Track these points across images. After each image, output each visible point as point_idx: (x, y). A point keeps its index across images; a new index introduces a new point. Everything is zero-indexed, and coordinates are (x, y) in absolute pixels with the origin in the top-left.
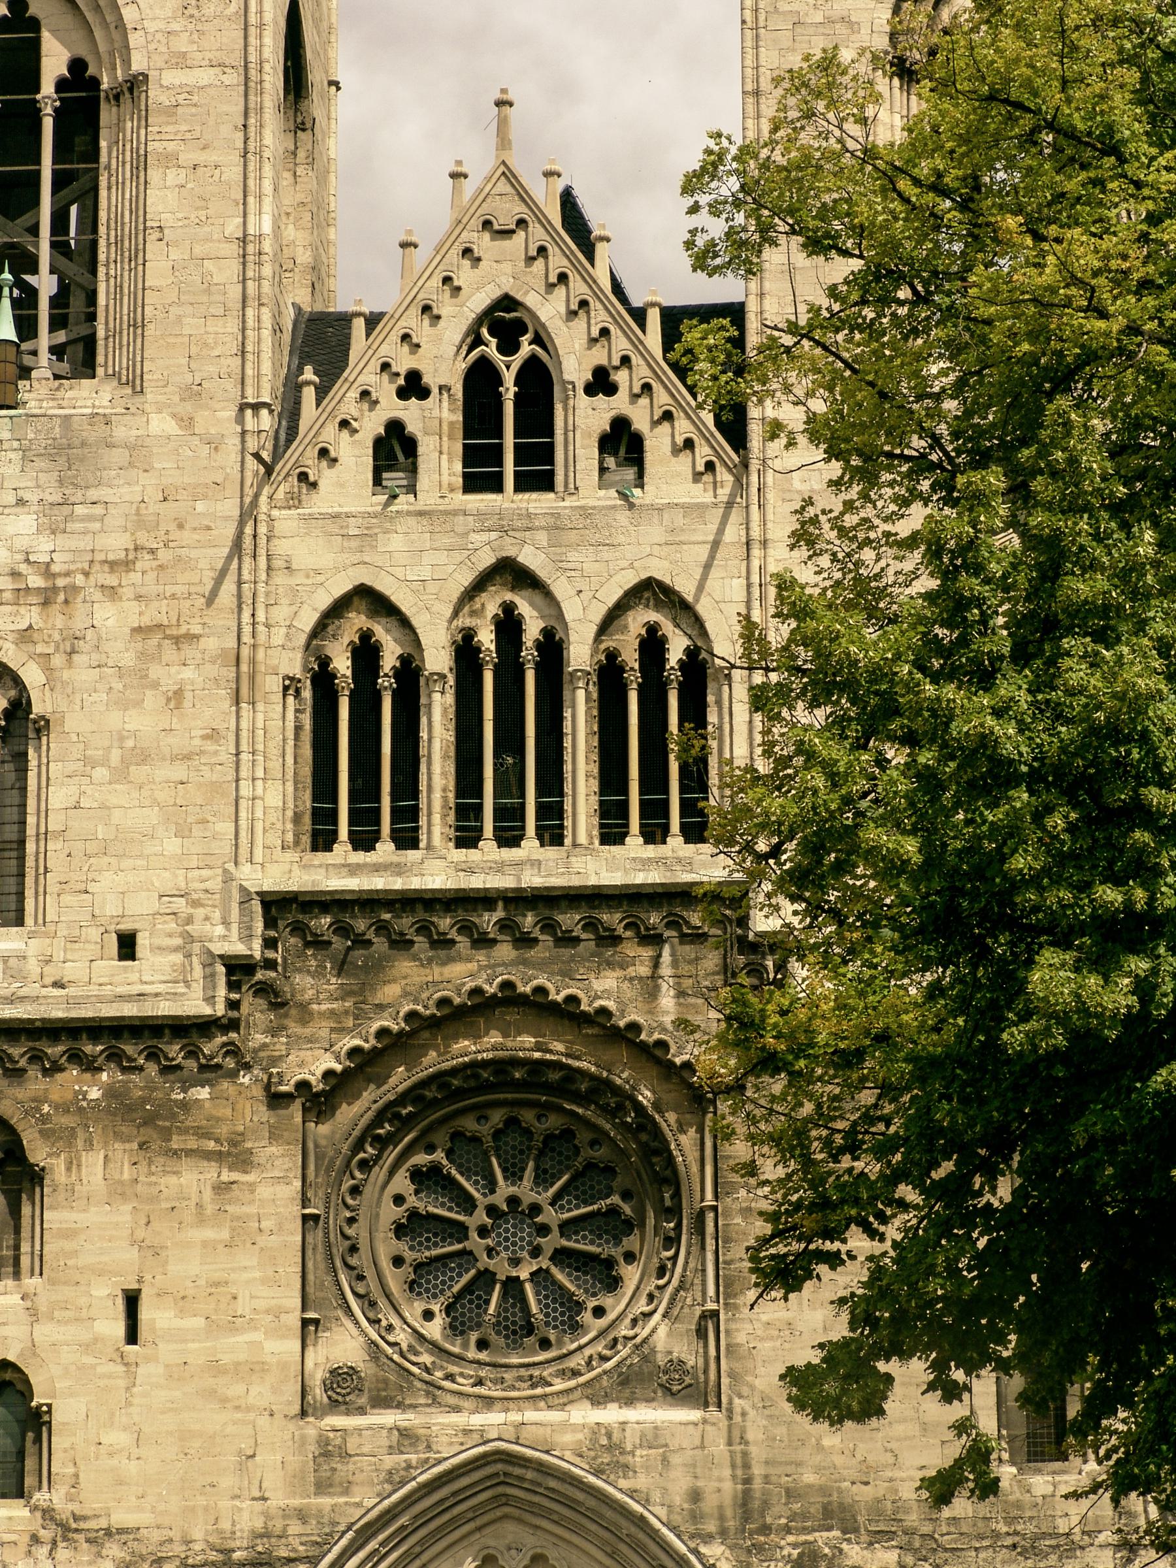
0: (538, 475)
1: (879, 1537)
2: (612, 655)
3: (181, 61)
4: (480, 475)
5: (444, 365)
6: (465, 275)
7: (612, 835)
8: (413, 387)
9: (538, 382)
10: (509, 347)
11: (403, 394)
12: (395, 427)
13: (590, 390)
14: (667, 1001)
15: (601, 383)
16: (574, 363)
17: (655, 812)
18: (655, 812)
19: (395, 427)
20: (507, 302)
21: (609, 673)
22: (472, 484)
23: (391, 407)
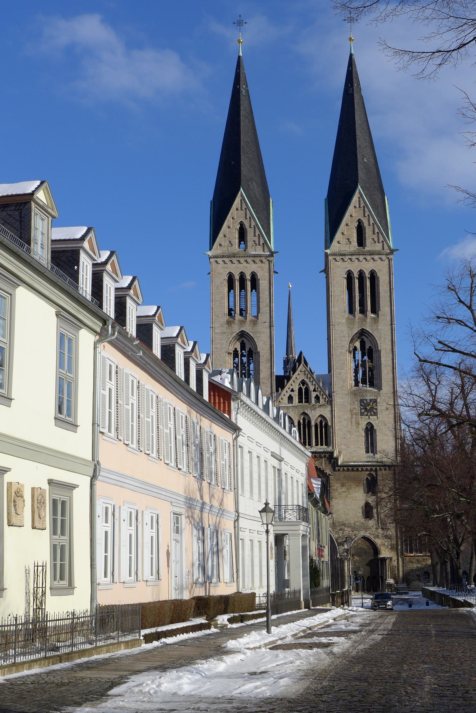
0: (308, 400)
1: (348, 527)
2: (316, 423)
4: (300, 401)
5: (296, 389)
6: (298, 377)
7: (317, 445)
8: (292, 390)
9: (307, 389)
10: (303, 385)
11: (291, 391)
12: (290, 395)
13: (313, 391)
14: (323, 465)
15: (314, 390)
16: (312, 388)
17: (322, 442)
18: (322, 442)
19: (290, 395)
20: (303, 380)
21: (316, 426)
22: (299, 402)
23: (290, 393)
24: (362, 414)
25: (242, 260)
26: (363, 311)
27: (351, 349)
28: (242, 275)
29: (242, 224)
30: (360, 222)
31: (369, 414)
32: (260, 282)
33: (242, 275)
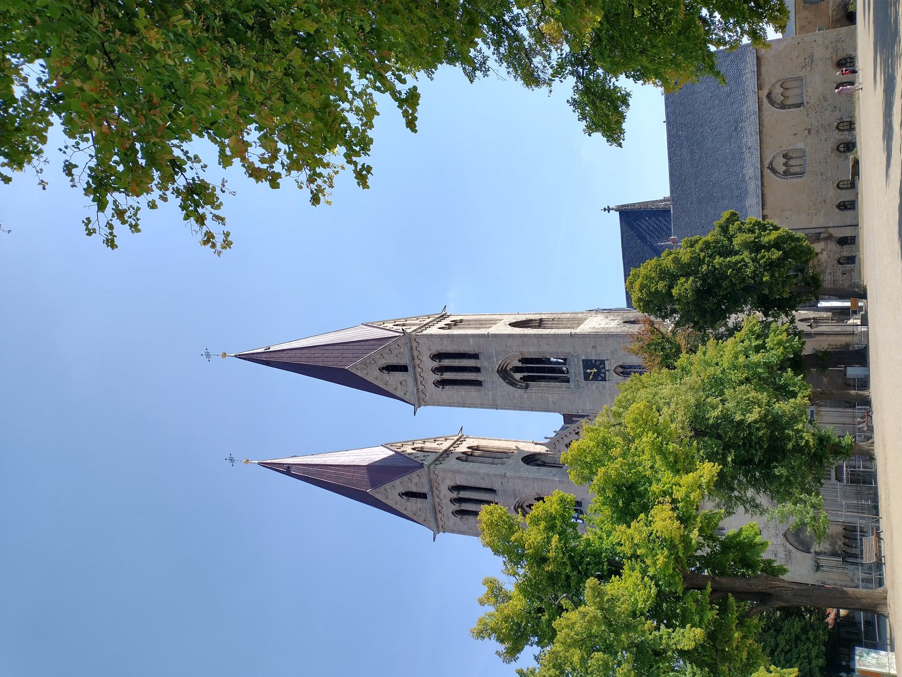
3: (534, 488)
24: (604, 379)
25: (437, 500)
26: (477, 370)
27: (524, 385)
28: (453, 501)
29: (402, 495)
30: (382, 369)
31: (603, 371)
32: (459, 483)
33: (453, 501)
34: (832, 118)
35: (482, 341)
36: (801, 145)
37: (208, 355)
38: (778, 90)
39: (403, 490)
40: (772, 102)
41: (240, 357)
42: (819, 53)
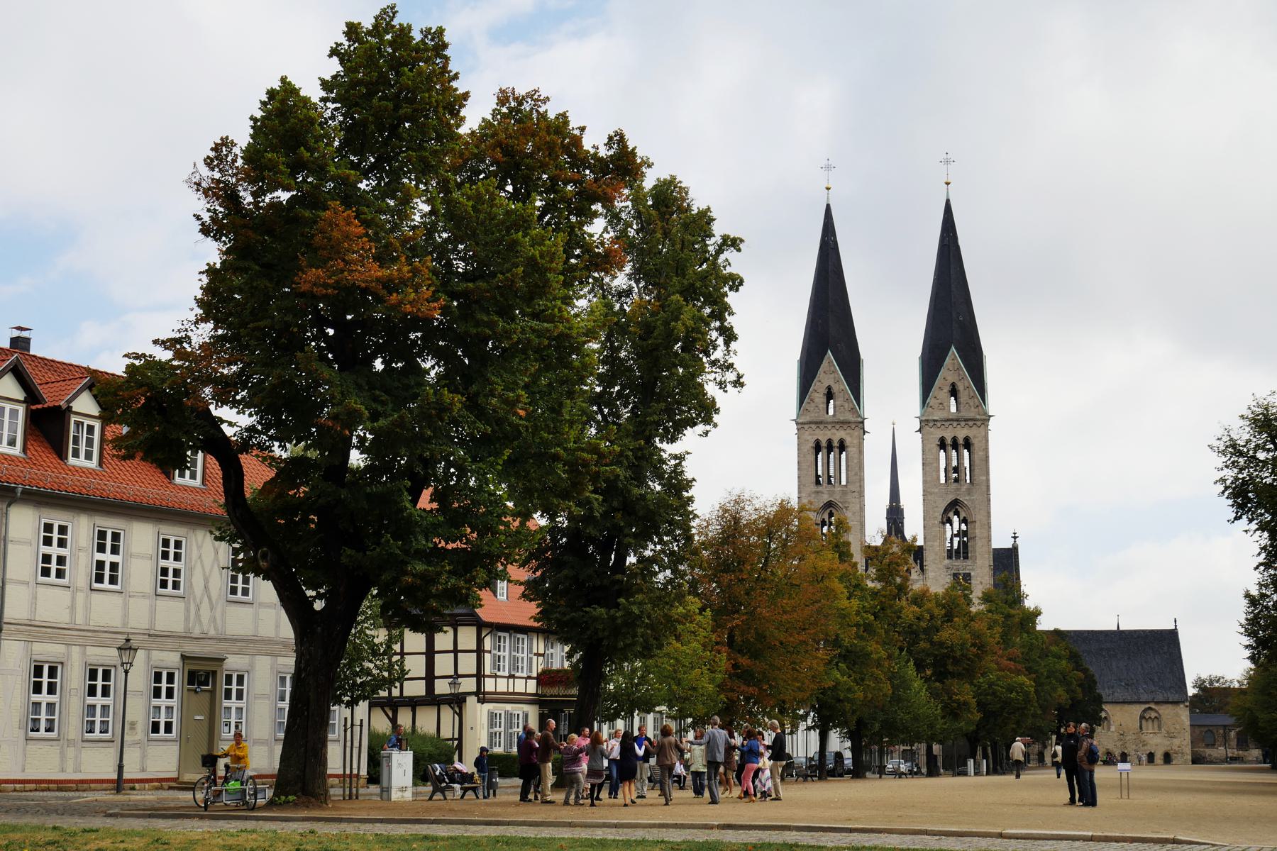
29: (829, 388)
34: (1130, 749)
35: (984, 488)
36: (1113, 729)
37: (947, 162)
38: (1153, 715)
39: (835, 389)
40: (1145, 711)
41: (948, 202)
42: (1176, 742)
